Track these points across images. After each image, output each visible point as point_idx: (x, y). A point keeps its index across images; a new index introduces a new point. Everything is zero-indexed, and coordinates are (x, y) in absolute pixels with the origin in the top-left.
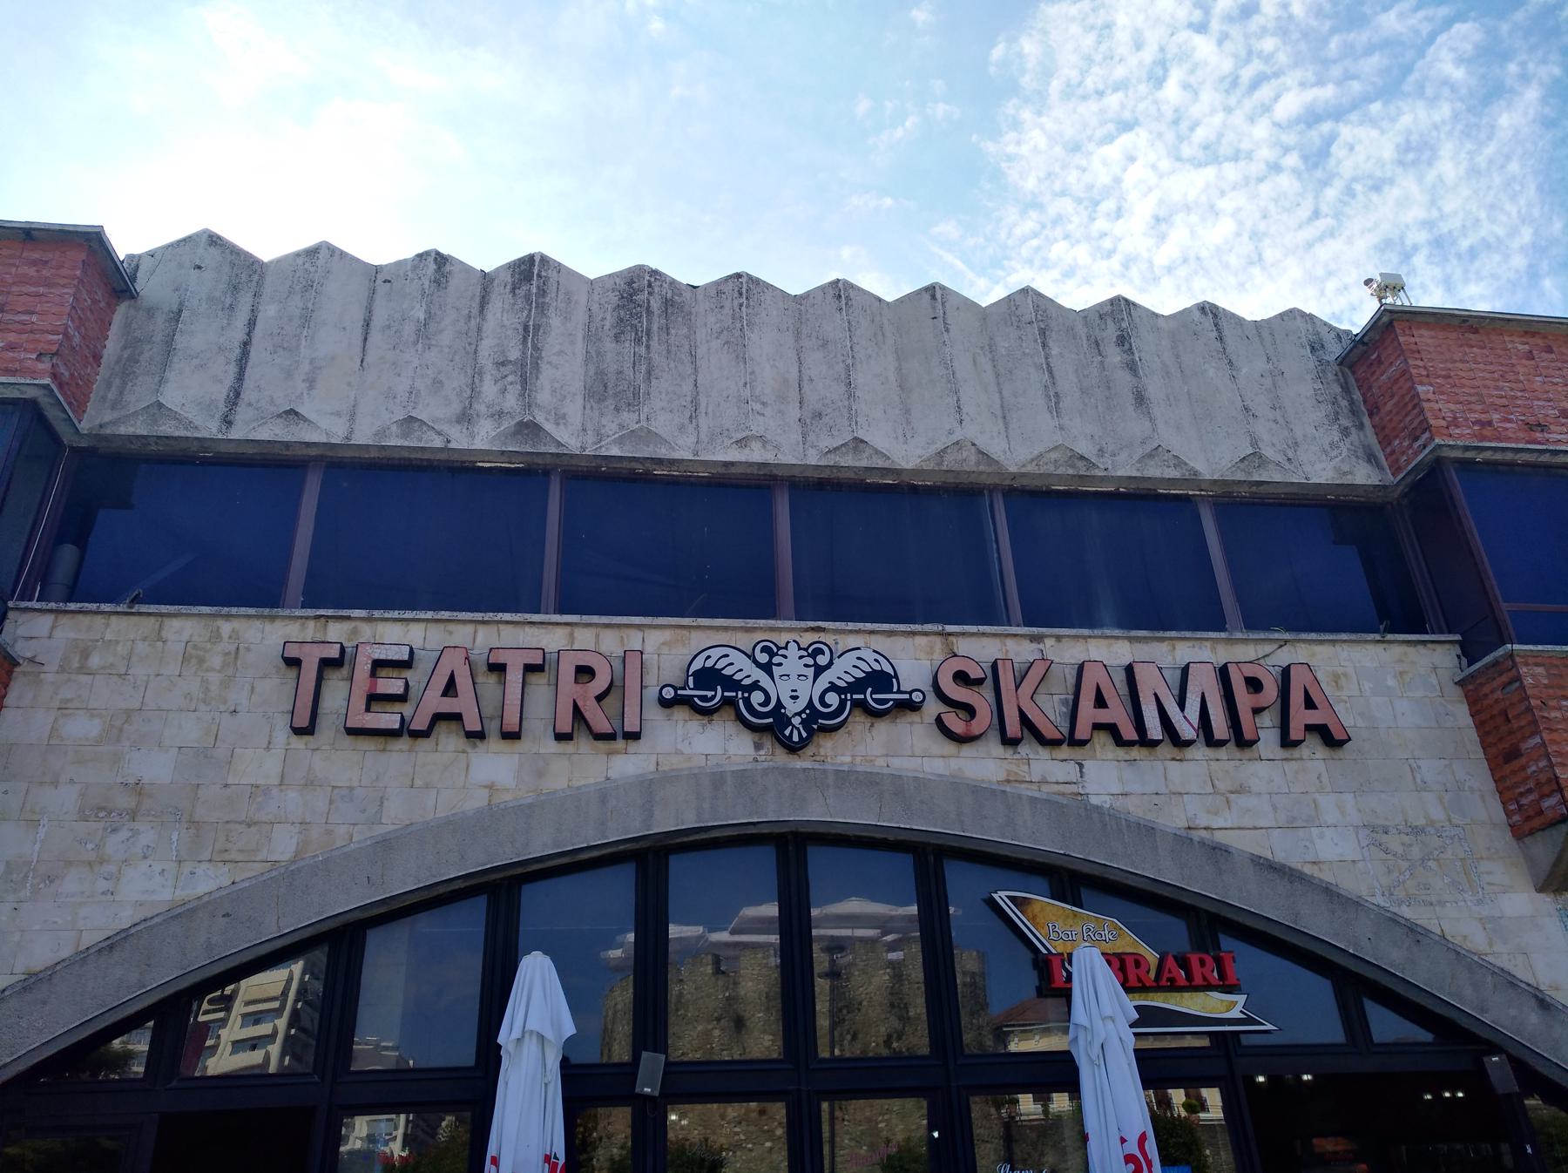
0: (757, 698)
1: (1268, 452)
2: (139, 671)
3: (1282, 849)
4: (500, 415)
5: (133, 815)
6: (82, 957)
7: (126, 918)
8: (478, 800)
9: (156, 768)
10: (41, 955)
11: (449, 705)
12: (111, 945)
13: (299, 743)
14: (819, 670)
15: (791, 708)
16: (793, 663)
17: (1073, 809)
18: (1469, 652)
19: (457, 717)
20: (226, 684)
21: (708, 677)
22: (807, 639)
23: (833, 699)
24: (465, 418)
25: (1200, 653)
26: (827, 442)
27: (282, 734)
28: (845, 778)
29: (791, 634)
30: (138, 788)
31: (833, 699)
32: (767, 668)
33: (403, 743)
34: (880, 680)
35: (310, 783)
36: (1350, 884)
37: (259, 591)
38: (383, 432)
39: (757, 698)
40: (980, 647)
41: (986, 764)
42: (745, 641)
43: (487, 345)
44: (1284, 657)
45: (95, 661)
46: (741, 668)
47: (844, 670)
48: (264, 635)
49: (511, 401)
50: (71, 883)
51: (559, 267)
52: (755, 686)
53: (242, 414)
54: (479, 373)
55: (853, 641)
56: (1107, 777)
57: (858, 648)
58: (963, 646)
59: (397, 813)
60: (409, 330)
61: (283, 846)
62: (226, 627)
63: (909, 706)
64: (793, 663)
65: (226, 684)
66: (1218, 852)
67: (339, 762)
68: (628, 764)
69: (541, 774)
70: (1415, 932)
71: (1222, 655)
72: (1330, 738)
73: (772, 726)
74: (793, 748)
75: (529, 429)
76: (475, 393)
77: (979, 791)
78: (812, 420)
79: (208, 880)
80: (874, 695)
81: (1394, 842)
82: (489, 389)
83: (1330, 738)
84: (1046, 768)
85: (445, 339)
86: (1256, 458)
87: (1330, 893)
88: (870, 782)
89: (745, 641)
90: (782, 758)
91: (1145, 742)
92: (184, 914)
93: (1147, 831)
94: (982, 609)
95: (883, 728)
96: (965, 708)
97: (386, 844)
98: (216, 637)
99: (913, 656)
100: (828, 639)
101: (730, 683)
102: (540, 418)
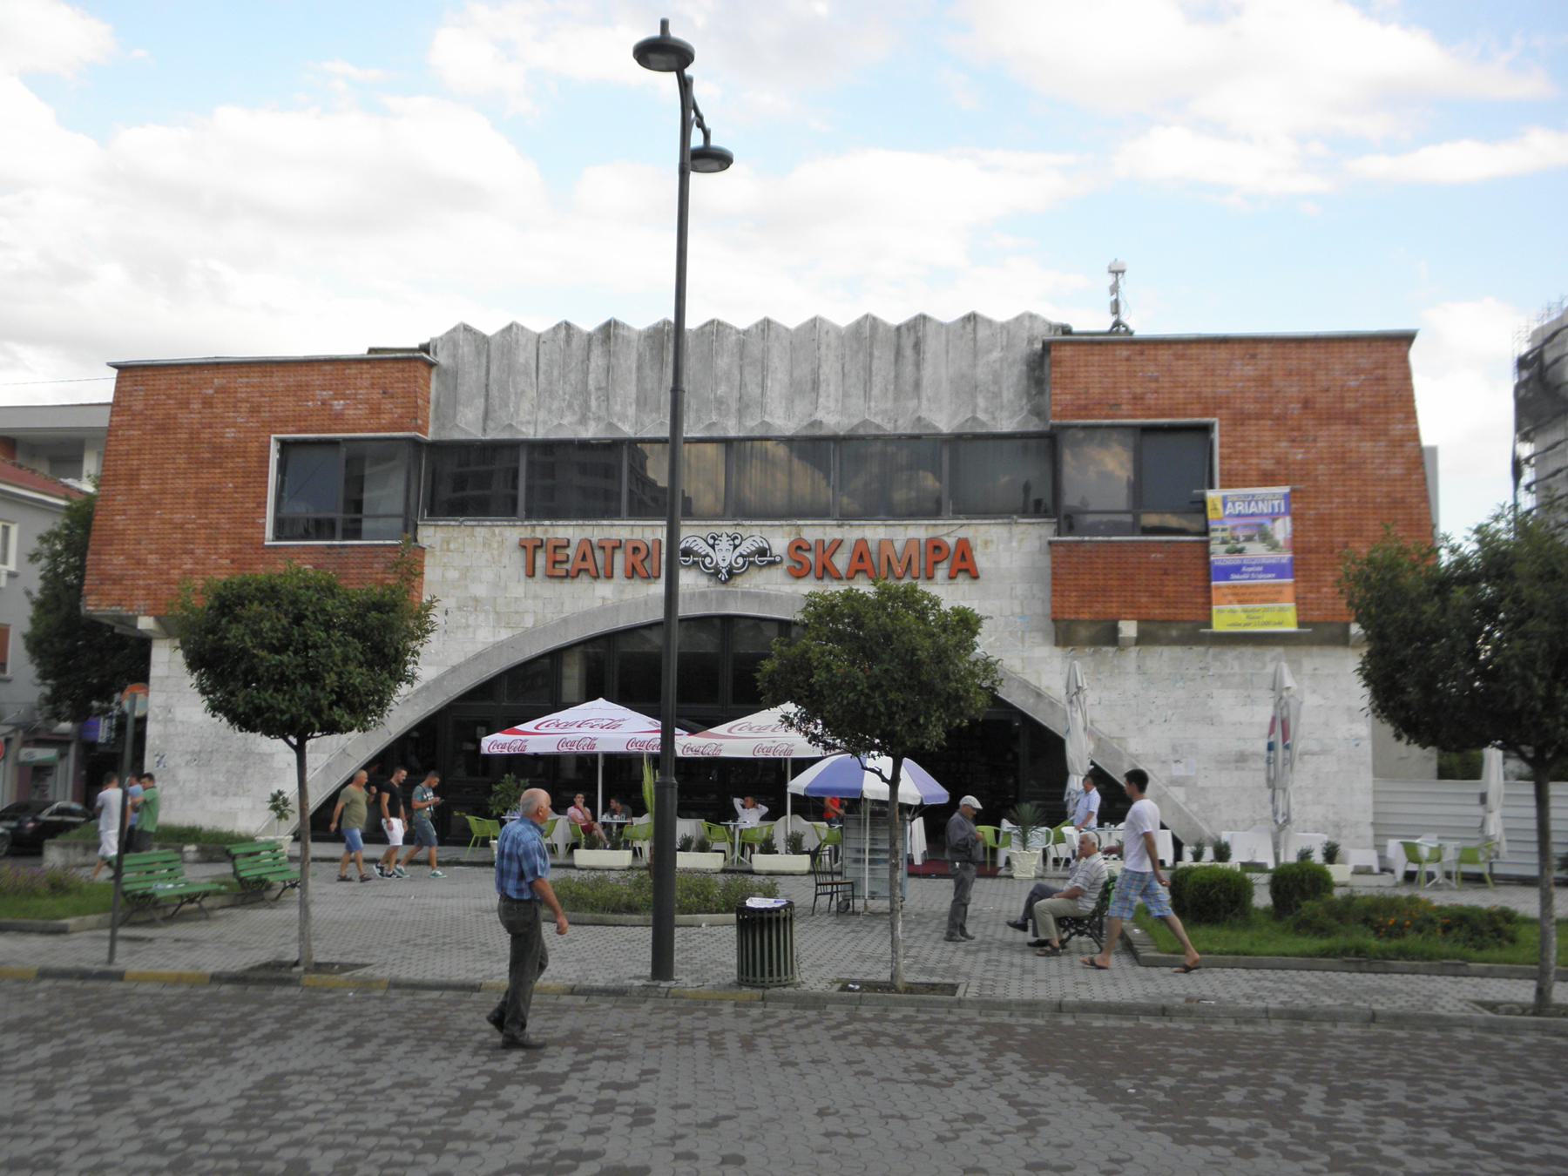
0: (708, 560)
2: (468, 550)
6: (468, 662)
7: (479, 648)
8: (598, 603)
9: (480, 590)
11: (584, 565)
12: (478, 656)
14: (736, 547)
15: (722, 564)
16: (724, 544)
19: (587, 570)
20: (500, 555)
22: (731, 531)
23: (741, 561)
28: (746, 595)
29: (726, 528)
30: (476, 599)
31: (741, 561)
32: (713, 547)
33: (568, 581)
34: (762, 552)
35: (535, 597)
37: (507, 509)
39: (708, 560)
40: (814, 532)
42: (704, 533)
43: (591, 377)
44: (963, 533)
45: (452, 546)
46: (701, 547)
47: (747, 547)
48: (511, 533)
49: (603, 413)
51: (624, 326)
52: (707, 555)
53: (491, 424)
54: (589, 394)
55: (756, 531)
57: (756, 534)
59: (569, 609)
61: (529, 622)
62: (497, 530)
63: (772, 563)
64: (724, 544)
65: (500, 555)
69: (622, 592)
72: (975, 577)
73: (715, 573)
74: (725, 582)
75: (611, 425)
76: (588, 408)
79: (504, 635)
89: (704, 533)
90: (723, 588)
92: (499, 647)
95: (765, 572)
98: (494, 534)
100: (740, 530)
102: (615, 420)
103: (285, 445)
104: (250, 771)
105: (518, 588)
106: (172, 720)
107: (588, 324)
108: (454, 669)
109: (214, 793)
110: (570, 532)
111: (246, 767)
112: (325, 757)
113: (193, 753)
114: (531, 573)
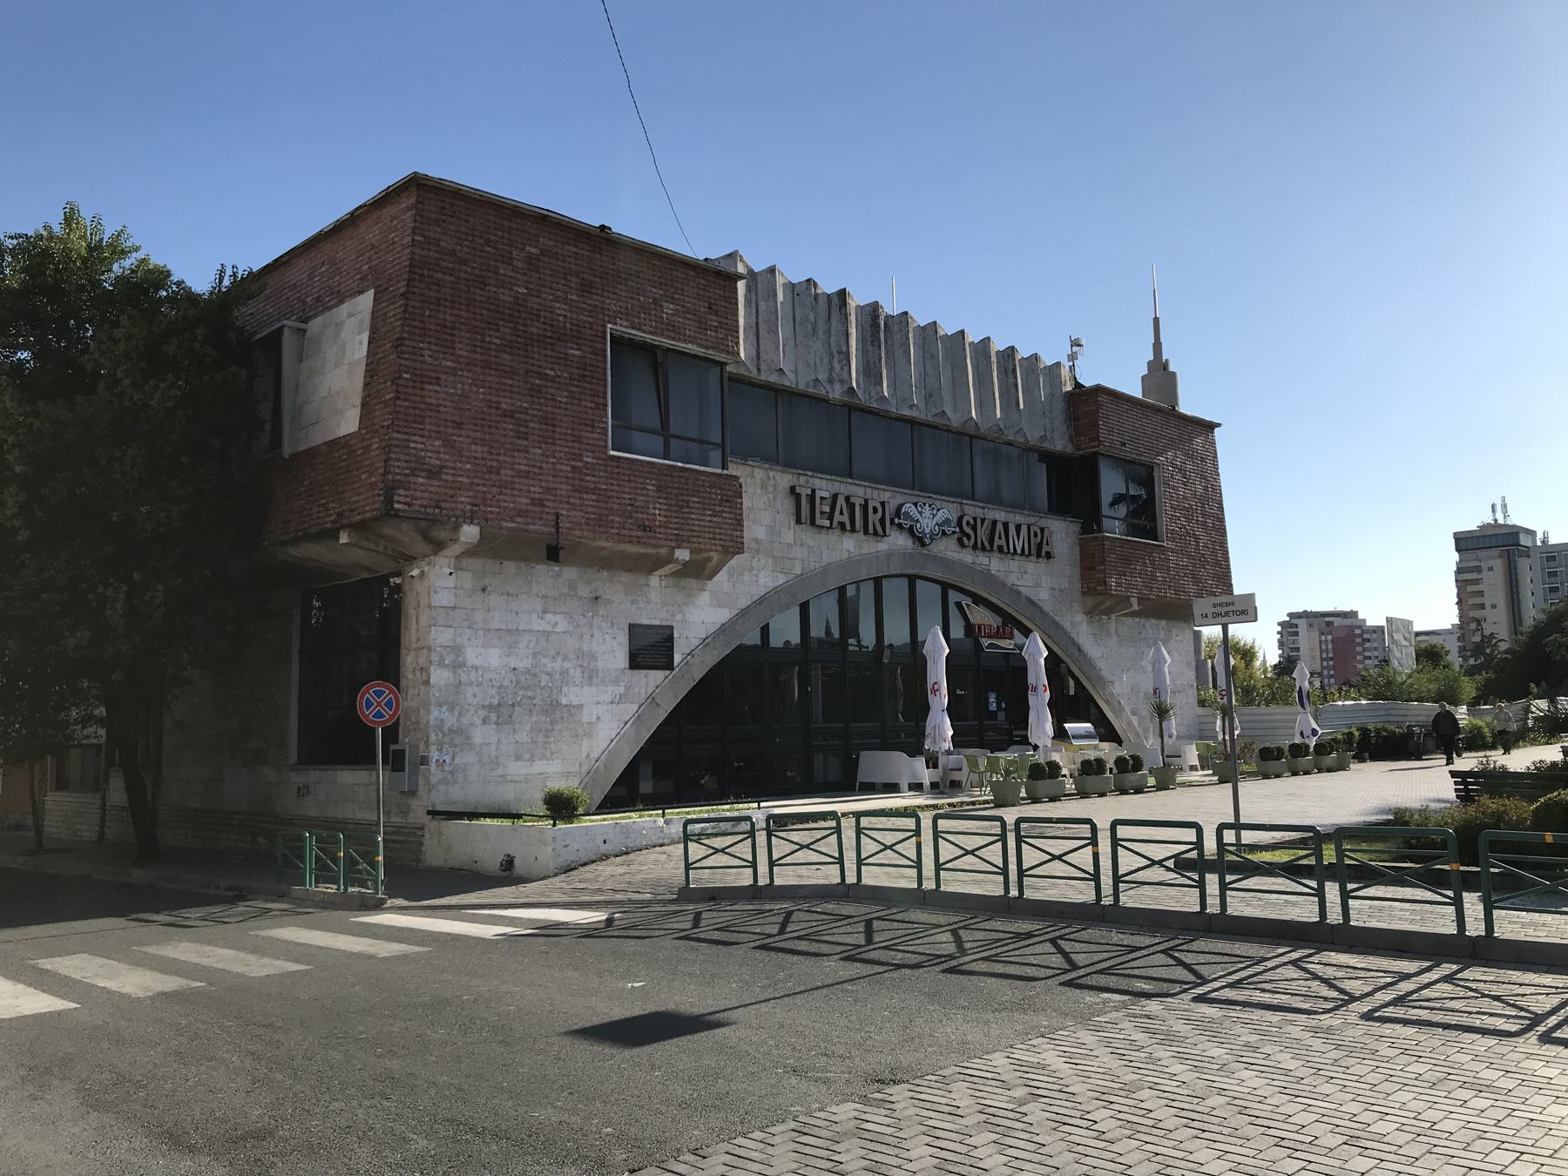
4: (842, 381)
5: (757, 551)
8: (845, 556)
10: (744, 602)
12: (762, 600)
13: (797, 527)
17: (987, 575)
18: (1086, 529)
24: (831, 381)
26: (934, 411)
27: (793, 523)
38: (807, 385)
41: (967, 556)
43: (833, 339)
48: (784, 479)
50: (746, 577)
54: (832, 356)
56: (994, 564)
58: (968, 510)
59: (826, 559)
60: (810, 328)
64: (927, 511)
67: (808, 536)
68: (882, 546)
71: (1032, 520)
72: (1049, 556)
76: (831, 369)
77: (969, 568)
78: (928, 397)
79: (781, 579)
82: (837, 366)
83: (1049, 556)
84: (982, 559)
85: (821, 334)
87: (1041, 610)
97: (826, 570)
101: (912, 519)
104: (557, 727)
105: (790, 533)
106: (463, 664)
107: (828, 287)
108: (744, 612)
109: (518, 758)
110: (825, 487)
111: (552, 723)
112: (635, 707)
113: (491, 706)
114: (798, 521)
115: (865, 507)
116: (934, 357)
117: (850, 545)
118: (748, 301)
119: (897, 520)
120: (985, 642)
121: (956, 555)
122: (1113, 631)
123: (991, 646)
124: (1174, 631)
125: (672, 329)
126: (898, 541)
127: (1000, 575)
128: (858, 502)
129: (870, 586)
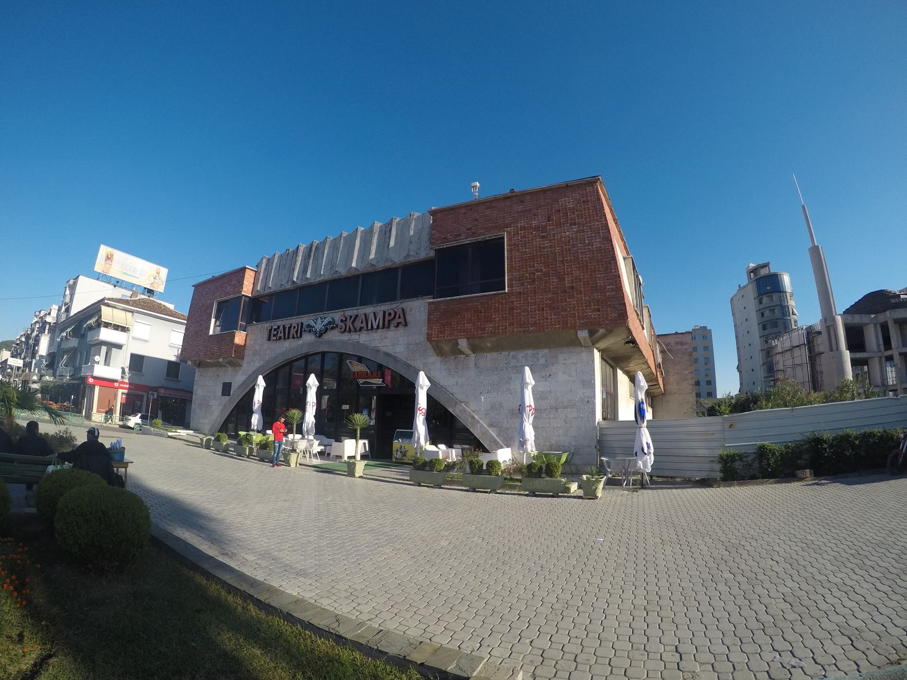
1: (411, 253)
3: (389, 350)
9: (257, 347)
10: (250, 373)
16: (319, 321)
21: (309, 326)
25: (381, 308)
36: (401, 357)
37: (266, 319)
40: (350, 312)
41: (346, 337)
46: (312, 323)
47: (326, 321)
56: (363, 338)
57: (329, 316)
64: (319, 321)
66: (378, 351)
68: (300, 342)
70: (409, 366)
80: (331, 326)
81: (411, 347)
84: (354, 336)
86: (408, 255)
88: (329, 343)
91: (368, 330)
93: (367, 348)
94: (353, 304)
96: (350, 326)
99: (337, 316)
103: (220, 304)
105: (267, 344)
114: (269, 339)
115: (290, 328)
116: (338, 249)
117: (286, 345)
118: (265, 269)
119: (300, 331)
120: (361, 381)
121: (338, 338)
122: (472, 365)
123: (364, 383)
124: (561, 357)
125: (229, 294)
126: (308, 338)
127: (366, 343)
128: (287, 326)
129: (318, 358)
